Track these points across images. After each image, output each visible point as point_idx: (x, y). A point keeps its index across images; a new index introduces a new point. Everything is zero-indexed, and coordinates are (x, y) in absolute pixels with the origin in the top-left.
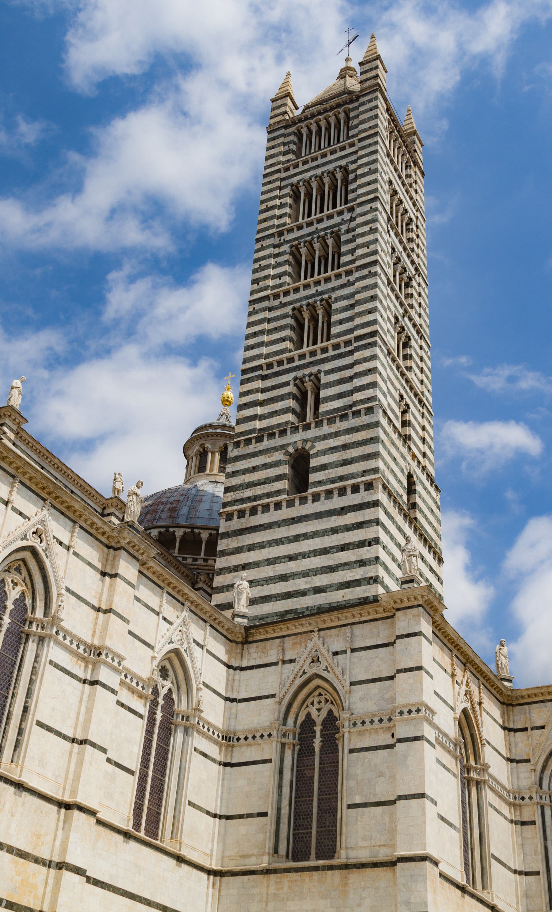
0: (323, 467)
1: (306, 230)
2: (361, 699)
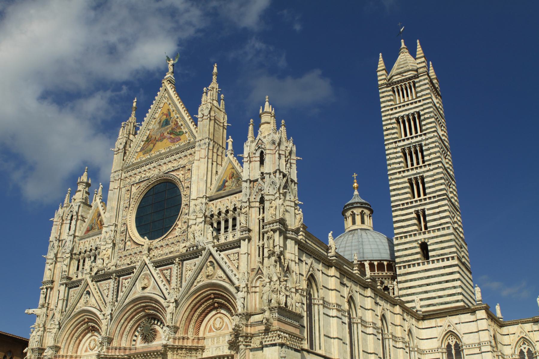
0: (434, 250)
1: (406, 142)
2: (467, 339)
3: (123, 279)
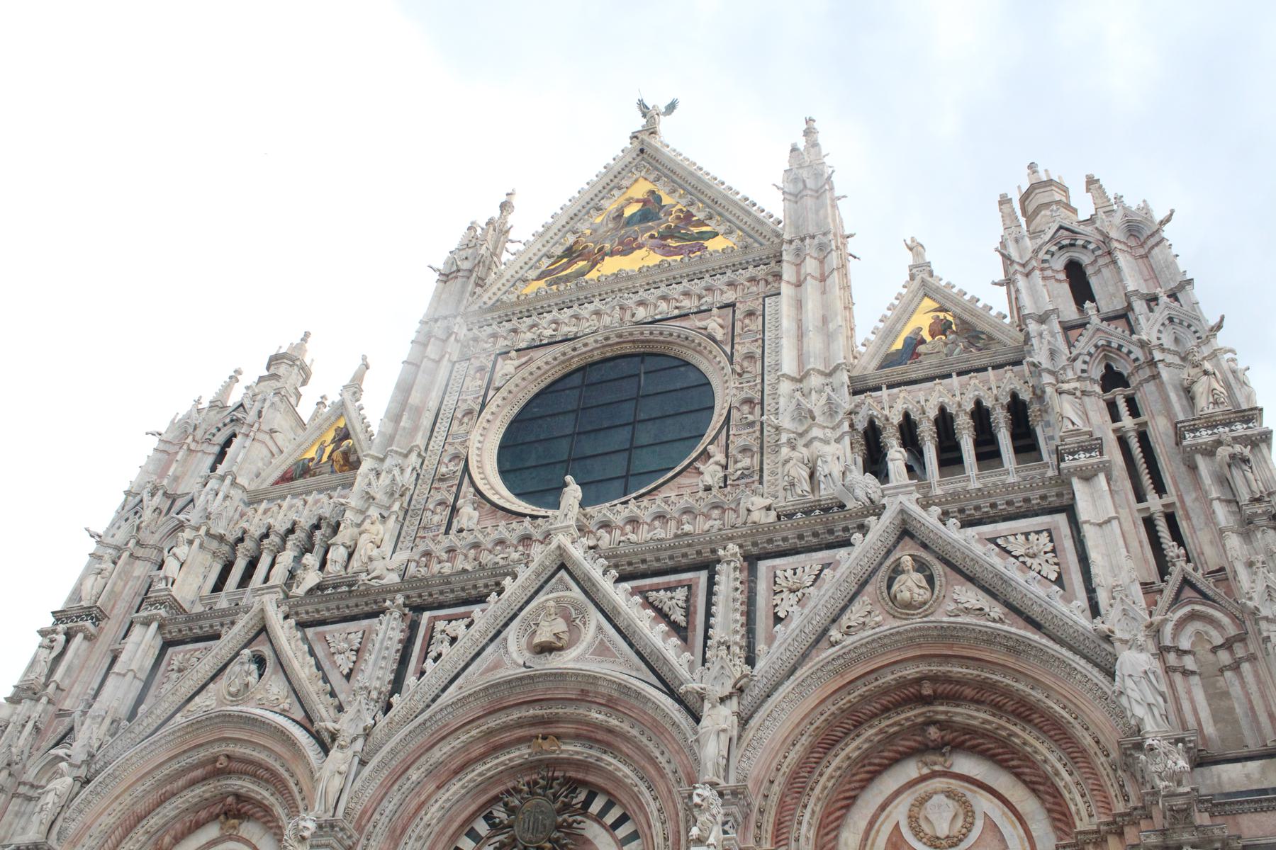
3: (436, 618)
